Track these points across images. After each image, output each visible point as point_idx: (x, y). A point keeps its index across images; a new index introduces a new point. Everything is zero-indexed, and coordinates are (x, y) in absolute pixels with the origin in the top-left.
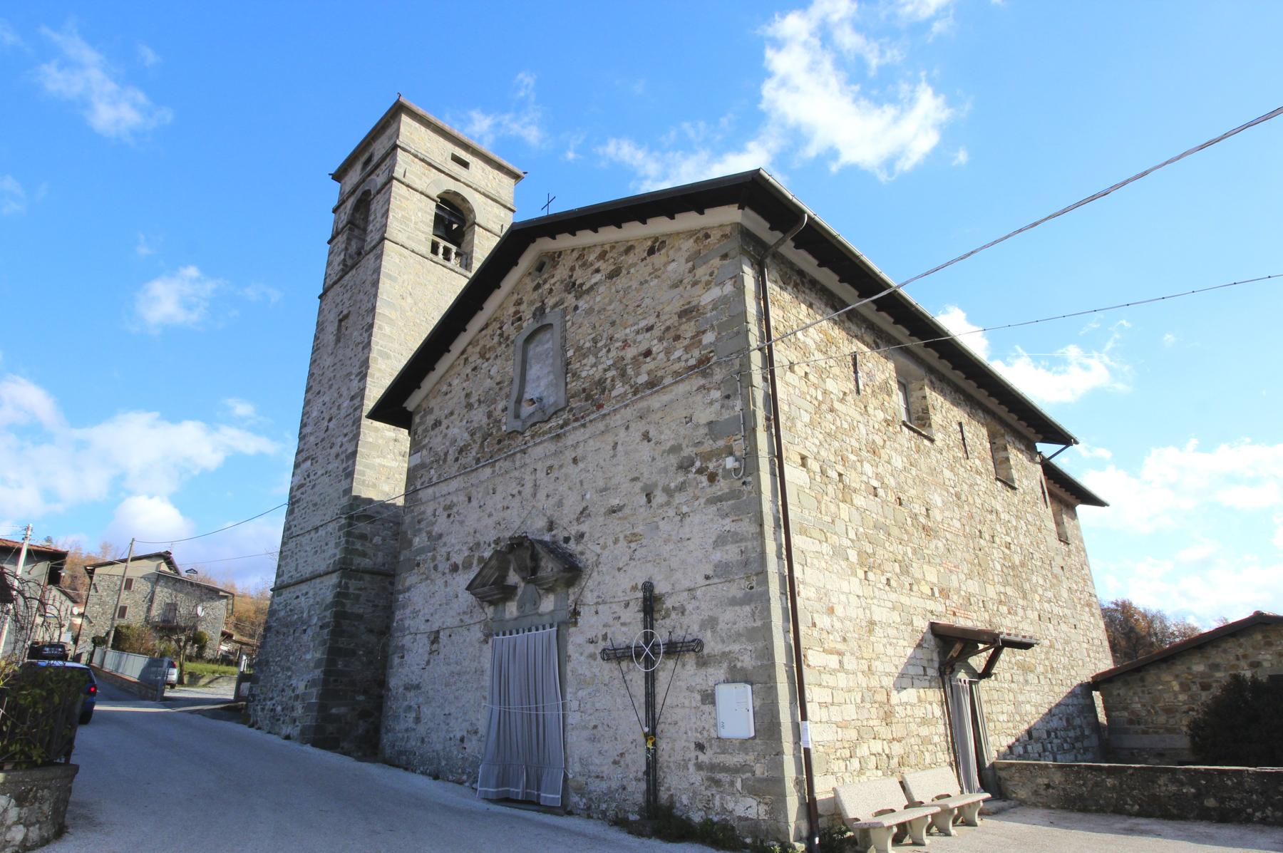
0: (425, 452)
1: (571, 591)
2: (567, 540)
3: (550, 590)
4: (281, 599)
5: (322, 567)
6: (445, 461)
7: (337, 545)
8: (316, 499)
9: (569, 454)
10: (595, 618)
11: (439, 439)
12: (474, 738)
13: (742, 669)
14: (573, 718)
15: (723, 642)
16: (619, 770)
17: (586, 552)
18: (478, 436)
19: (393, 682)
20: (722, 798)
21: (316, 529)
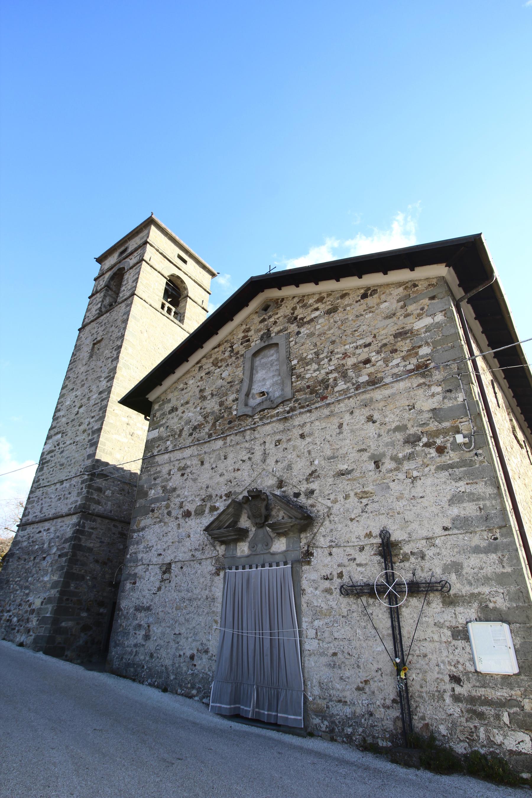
0: (162, 429)
1: (302, 536)
2: (297, 495)
3: (284, 534)
4: (25, 533)
5: (65, 510)
6: (180, 435)
7: (79, 494)
8: (63, 461)
9: (297, 432)
10: (329, 558)
11: (176, 420)
12: (205, 657)
13: (495, 609)
14: (310, 645)
15: (471, 584)
16: (364, 697)
17: (320, 505)
18: (210, 419)
19: (124, 604)
20: (486, 731)
21: (62, 482)
